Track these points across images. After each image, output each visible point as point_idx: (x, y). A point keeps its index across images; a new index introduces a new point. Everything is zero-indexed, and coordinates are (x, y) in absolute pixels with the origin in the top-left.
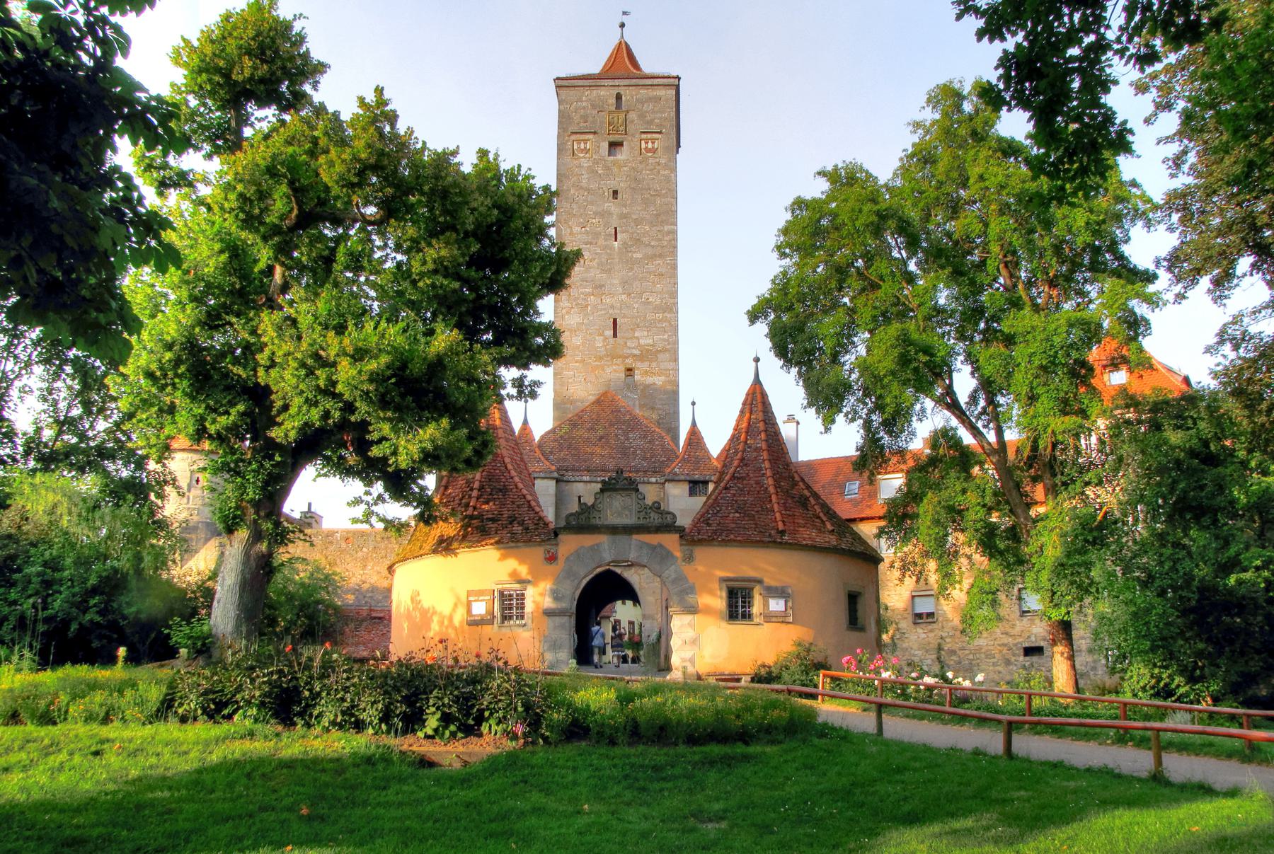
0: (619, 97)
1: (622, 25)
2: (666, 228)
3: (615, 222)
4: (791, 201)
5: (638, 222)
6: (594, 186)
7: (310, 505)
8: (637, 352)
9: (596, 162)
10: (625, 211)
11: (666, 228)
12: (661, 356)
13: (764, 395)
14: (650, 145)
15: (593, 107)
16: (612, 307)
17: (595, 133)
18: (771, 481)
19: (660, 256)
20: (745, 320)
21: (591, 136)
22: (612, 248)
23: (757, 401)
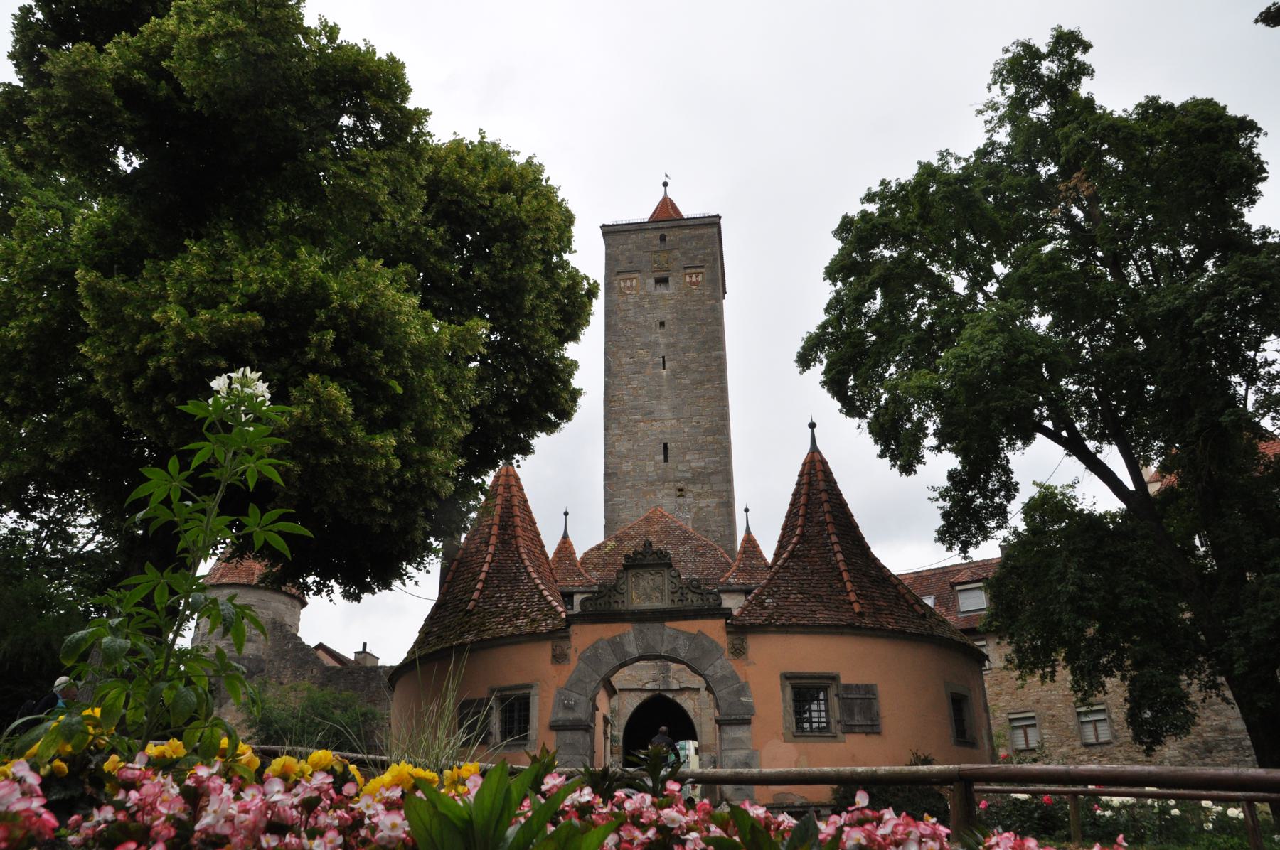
0: (663, 238)
1: (665, 184)
2: (714, 354)
3: (662, 351)
4: (835, 224)
5: (685, 350)
6: (641, 319)
7: (365, 645)
8: (689, 475)
9: (642, 298)
10: (672, 340)
11: (714, 354)
12: (713, 478)
13: (824, 463)
14: (694, 279)
15: (639, 248)
16: (662, 432)
17: (639, 271)
18: (840, 557)
19: (708, 381)
20: (795, 368)
21: (636, 275)
22: (660, 376)
23: (816, 483)
